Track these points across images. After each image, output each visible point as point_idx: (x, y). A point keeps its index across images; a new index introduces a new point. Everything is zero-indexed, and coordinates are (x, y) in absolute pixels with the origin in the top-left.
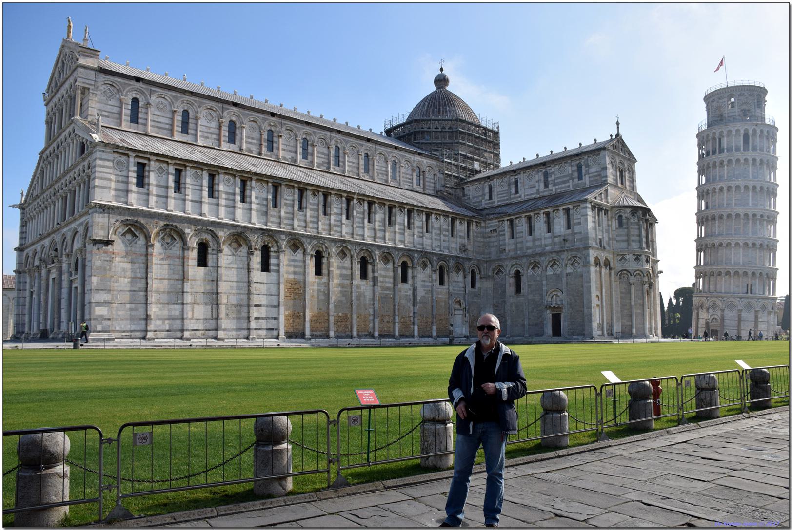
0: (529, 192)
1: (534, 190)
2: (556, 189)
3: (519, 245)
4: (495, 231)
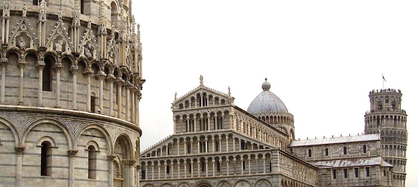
0: (335, 155)
1: (338, 155)
2: (351, 156)
3: (339, 182)
4: (325, 174)
